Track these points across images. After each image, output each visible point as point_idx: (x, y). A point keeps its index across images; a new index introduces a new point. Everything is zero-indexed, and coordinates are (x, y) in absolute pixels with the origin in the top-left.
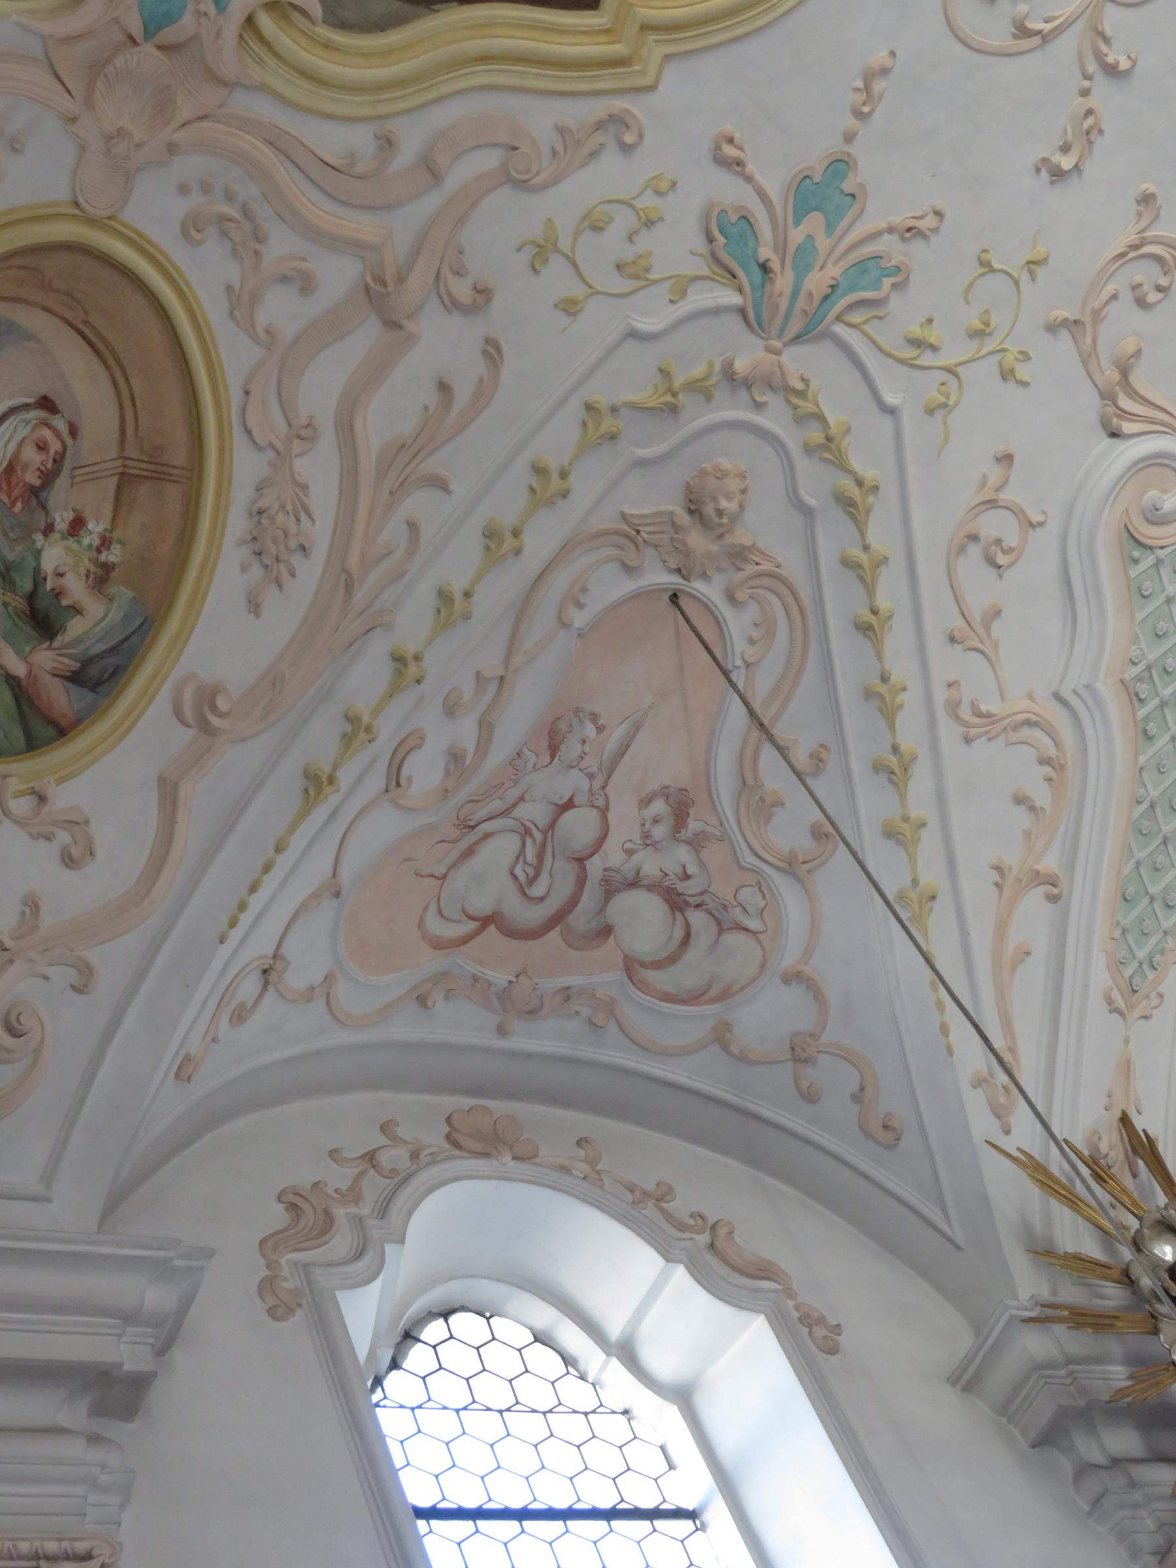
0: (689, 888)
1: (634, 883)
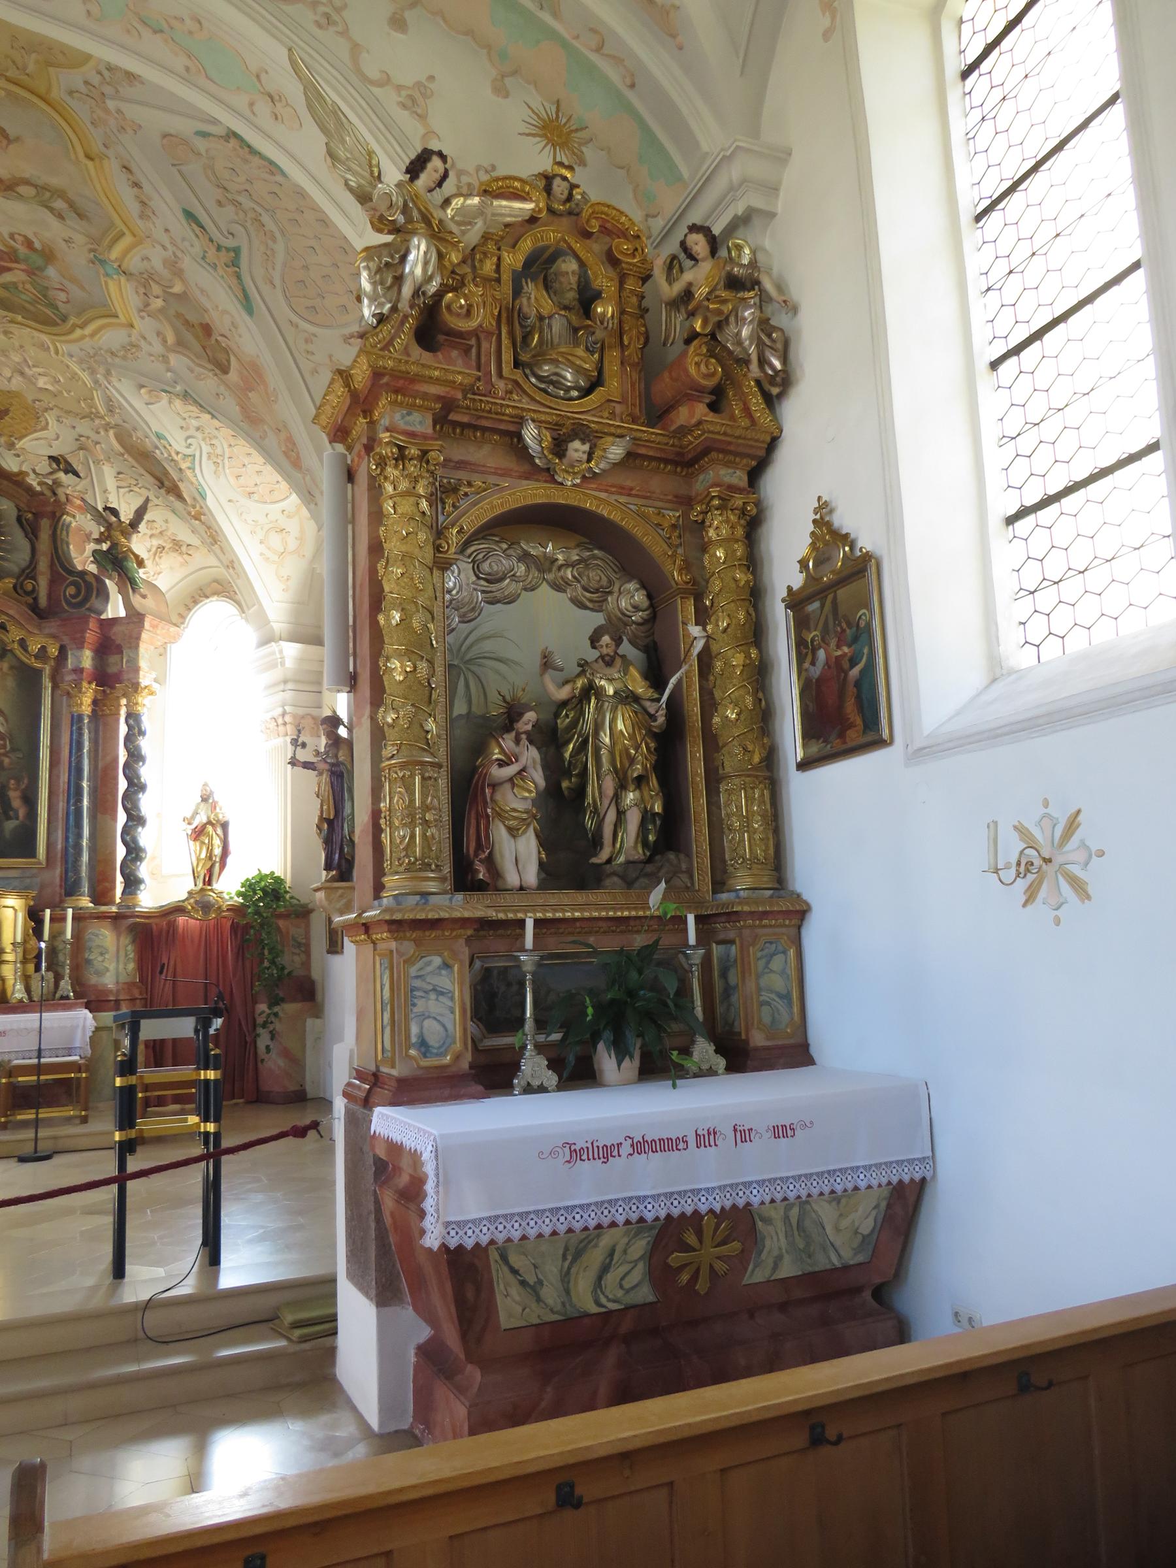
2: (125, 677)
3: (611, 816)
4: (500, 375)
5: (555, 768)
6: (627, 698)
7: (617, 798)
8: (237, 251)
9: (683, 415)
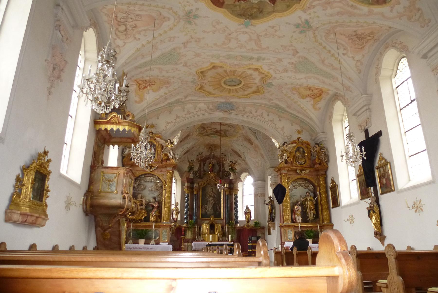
0: (127, 30)
1: (126, 26)
2: (234, 188)
3: (309, 214)
4: (294, 163)
5: (303, 208)
6: (311, 200)
7: (310, 212)
8: (256, 132)
9: (316, 166)
